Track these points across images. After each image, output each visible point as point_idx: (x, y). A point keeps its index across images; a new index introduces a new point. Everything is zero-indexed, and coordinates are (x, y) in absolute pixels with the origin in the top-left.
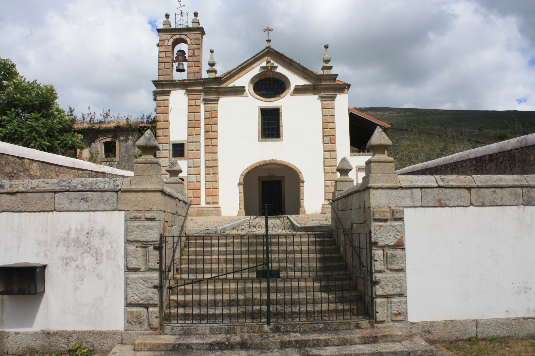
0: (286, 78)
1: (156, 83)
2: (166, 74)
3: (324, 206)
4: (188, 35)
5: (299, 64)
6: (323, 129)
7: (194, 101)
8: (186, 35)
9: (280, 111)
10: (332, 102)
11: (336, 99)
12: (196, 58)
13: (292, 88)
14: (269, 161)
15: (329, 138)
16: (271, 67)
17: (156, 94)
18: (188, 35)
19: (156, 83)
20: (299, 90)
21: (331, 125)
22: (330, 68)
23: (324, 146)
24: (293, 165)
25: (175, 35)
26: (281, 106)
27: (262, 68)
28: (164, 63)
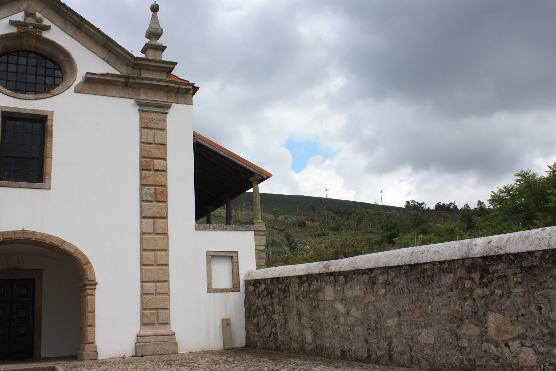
0: (67, 55)
3: (141, 339)
5: (98, 30)
6: (142, 169)
9: (49, 123)
10: (161, 117)
11: (170, 111)
13: (79, 78)
14: (15, 232)
15: (153, 192)
16: (35, 27)
20: (93, 83)
21: (158, 164)
22: (162, 48)
23: (141, 207)
24: (71, 245)
26: (52, 113)
27: (12, 23)
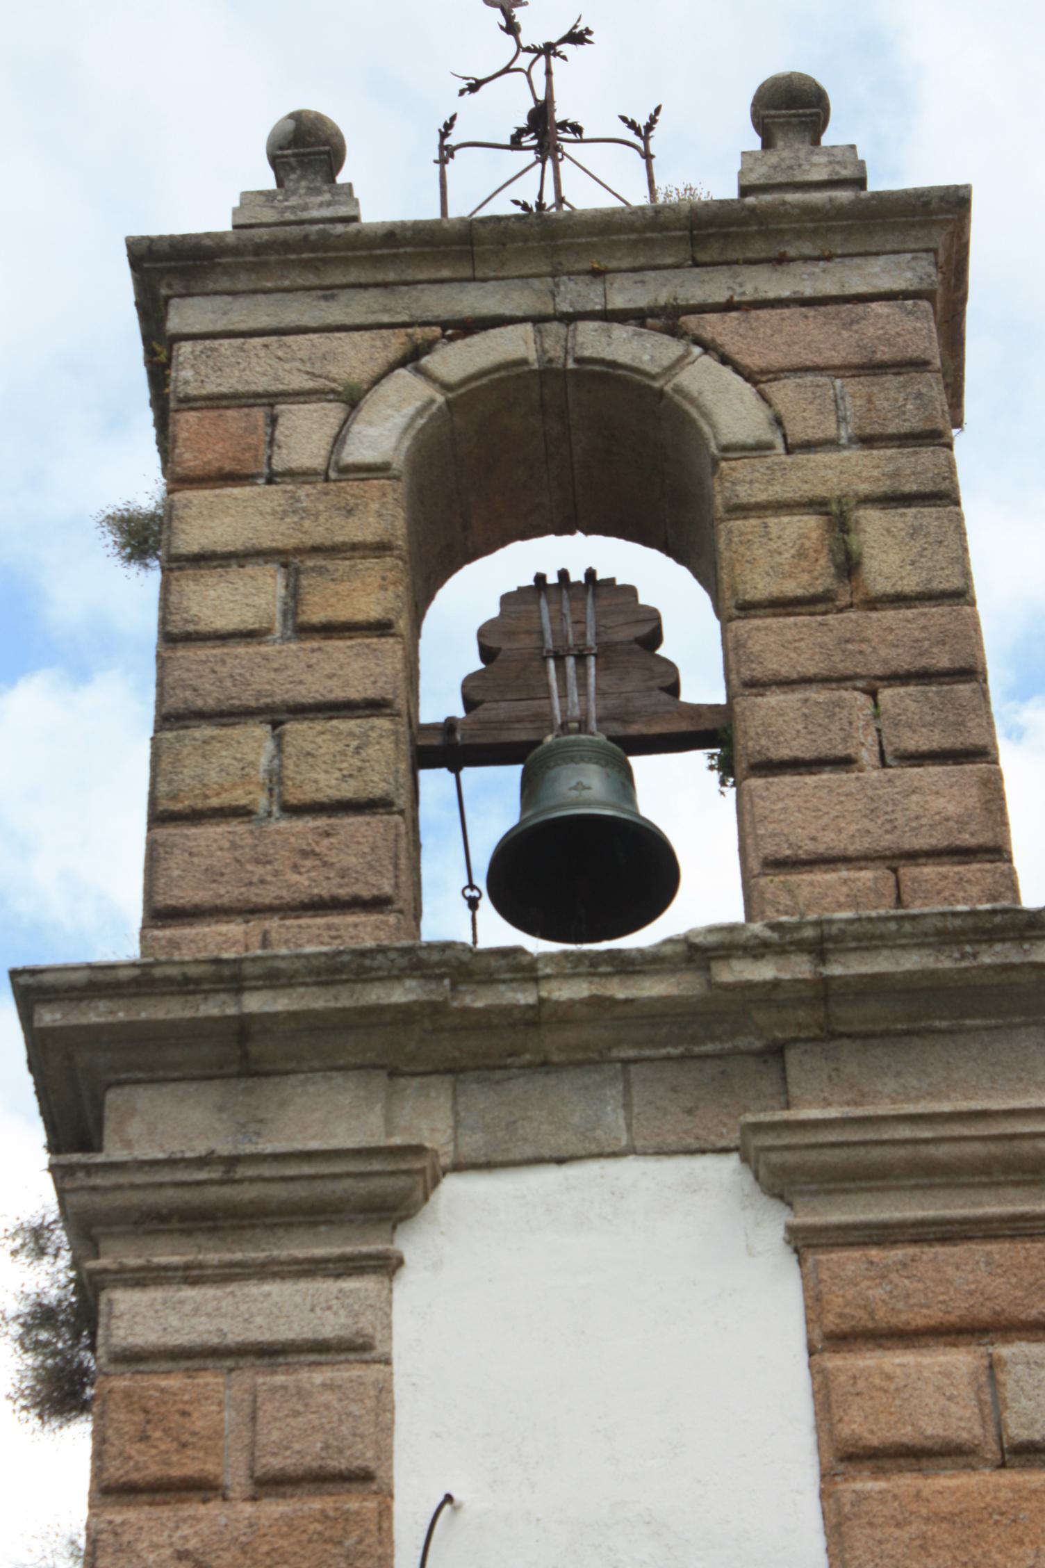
1: (90, 1048)
2: (308, 883)
4: (713, 326)
7: (960, 1360)
8: (668, 320)
12: (891, 638)
17: (111, 1216)
18: (713, 326)
19: (90, 1048)
25: (467, 327)
28: (278, 715)
